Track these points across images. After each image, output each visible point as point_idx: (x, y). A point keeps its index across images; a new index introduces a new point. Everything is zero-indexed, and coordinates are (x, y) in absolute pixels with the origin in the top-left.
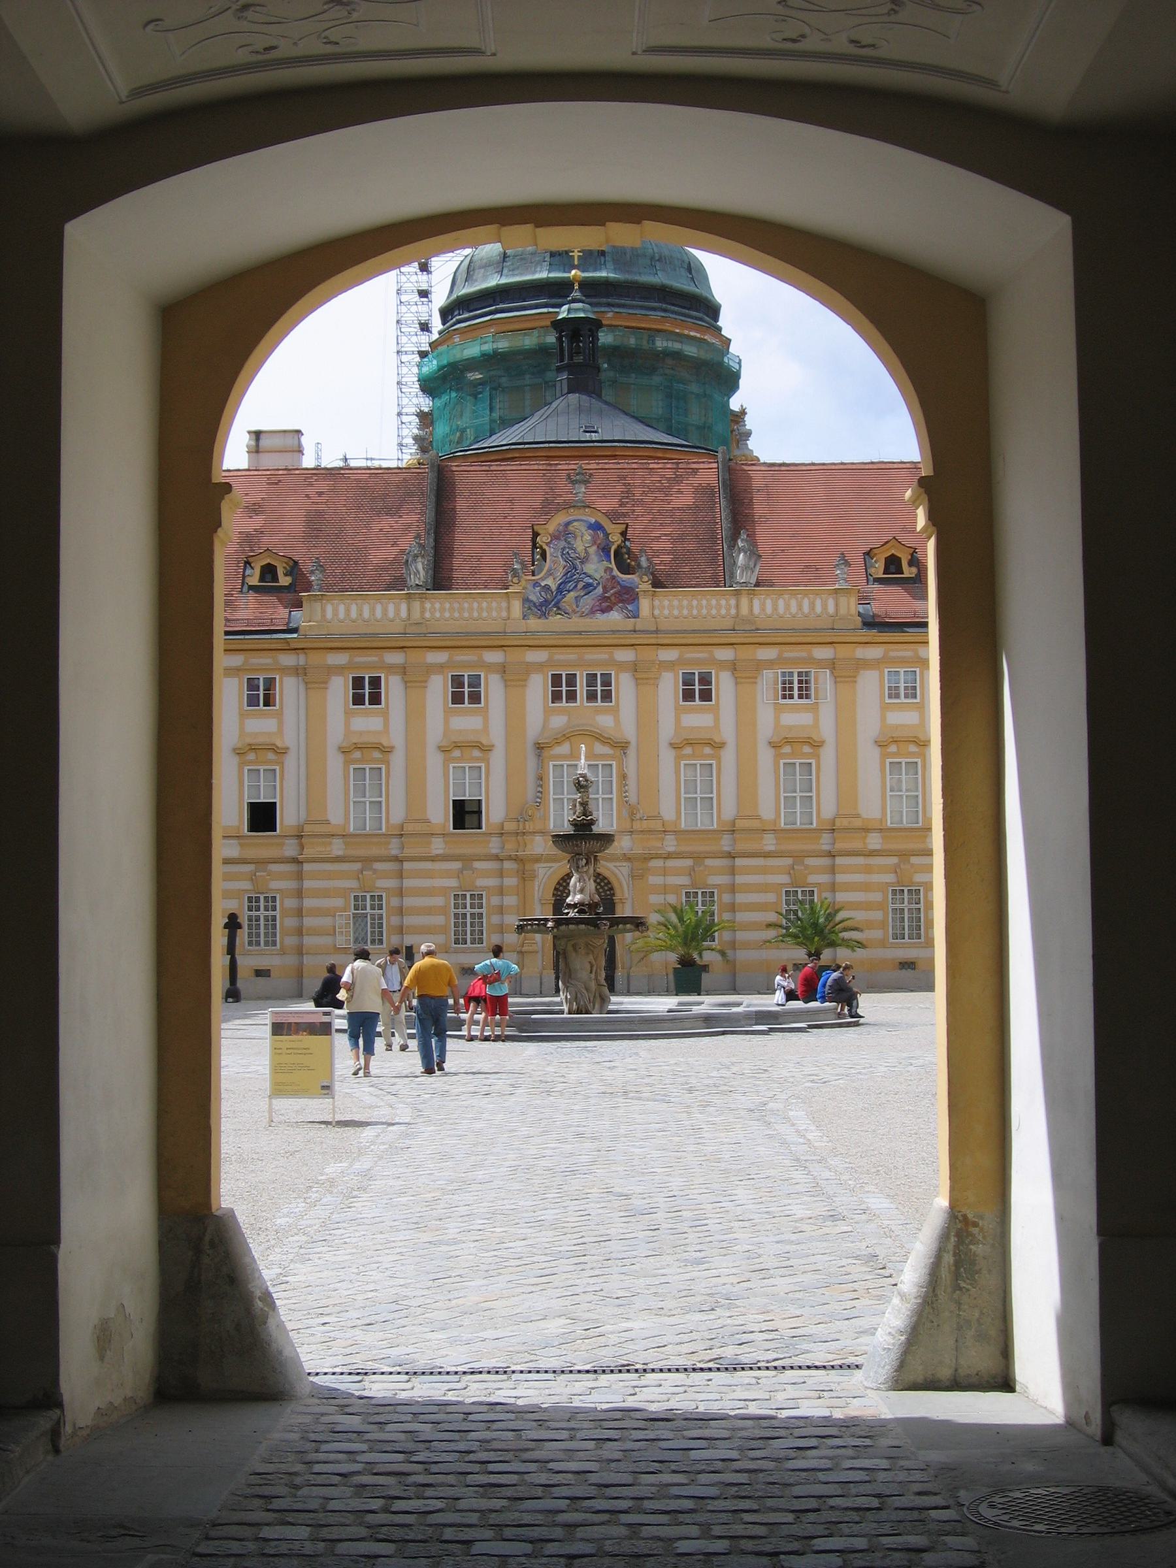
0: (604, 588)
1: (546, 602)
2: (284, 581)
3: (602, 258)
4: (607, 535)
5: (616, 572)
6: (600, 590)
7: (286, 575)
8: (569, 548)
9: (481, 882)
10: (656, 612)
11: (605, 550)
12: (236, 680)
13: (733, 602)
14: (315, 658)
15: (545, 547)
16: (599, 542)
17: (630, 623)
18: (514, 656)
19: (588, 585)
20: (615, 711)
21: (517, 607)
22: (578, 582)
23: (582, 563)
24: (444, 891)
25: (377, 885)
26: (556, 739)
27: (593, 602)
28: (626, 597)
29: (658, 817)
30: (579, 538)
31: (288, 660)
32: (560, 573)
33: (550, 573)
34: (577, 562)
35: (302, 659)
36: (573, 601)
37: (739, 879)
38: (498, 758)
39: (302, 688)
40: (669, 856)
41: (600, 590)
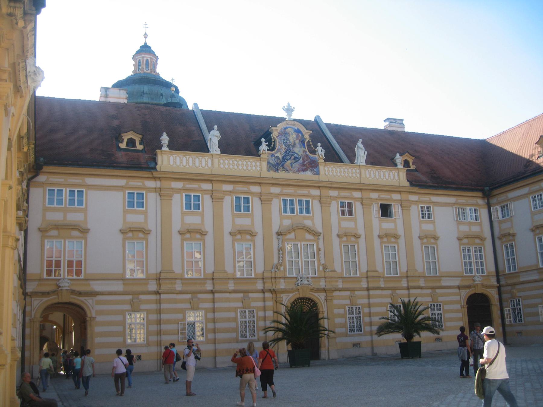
0: (303, 160)
1: (278, 164)
2: (140, 147)
3: (162, 97)
4: (303, 136)
5: (308, 153)
6: (301, 161)
7: (140, 144)
8: (287, 140)
9: (253, 304)
10: (327, 173)
11: (302, 142)
12: (121, 193)
13: (358, 171)
14: (166, 184)
15: (275, 138)
16: (300, 138)
17: (315, 178)
18: (265, 189)
19: (295, 158)
20: (312, 218)
21: (265, 165)
22: (291, 156)
23: (293, 147)
24: (235, 309)
25: (200, 306)
26: (289, 230)
27: (299, 166)
28: (313, 165)
29: (333, 271)
30: (291, 136)
31: (151, 184)
32: (283, 151)
33: (279, 151)
34: (291, 147)
35: (158, 184)
36: (290, 165)
37: (372, 301)
38: (259, 239)
39: (159, 198)
40: (340, 290)
41: (301, 161)
